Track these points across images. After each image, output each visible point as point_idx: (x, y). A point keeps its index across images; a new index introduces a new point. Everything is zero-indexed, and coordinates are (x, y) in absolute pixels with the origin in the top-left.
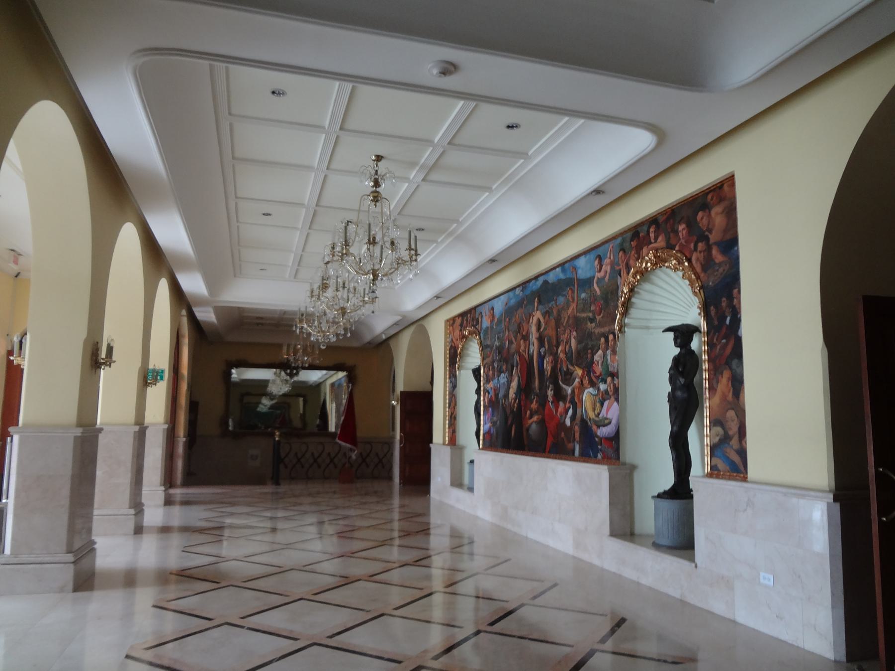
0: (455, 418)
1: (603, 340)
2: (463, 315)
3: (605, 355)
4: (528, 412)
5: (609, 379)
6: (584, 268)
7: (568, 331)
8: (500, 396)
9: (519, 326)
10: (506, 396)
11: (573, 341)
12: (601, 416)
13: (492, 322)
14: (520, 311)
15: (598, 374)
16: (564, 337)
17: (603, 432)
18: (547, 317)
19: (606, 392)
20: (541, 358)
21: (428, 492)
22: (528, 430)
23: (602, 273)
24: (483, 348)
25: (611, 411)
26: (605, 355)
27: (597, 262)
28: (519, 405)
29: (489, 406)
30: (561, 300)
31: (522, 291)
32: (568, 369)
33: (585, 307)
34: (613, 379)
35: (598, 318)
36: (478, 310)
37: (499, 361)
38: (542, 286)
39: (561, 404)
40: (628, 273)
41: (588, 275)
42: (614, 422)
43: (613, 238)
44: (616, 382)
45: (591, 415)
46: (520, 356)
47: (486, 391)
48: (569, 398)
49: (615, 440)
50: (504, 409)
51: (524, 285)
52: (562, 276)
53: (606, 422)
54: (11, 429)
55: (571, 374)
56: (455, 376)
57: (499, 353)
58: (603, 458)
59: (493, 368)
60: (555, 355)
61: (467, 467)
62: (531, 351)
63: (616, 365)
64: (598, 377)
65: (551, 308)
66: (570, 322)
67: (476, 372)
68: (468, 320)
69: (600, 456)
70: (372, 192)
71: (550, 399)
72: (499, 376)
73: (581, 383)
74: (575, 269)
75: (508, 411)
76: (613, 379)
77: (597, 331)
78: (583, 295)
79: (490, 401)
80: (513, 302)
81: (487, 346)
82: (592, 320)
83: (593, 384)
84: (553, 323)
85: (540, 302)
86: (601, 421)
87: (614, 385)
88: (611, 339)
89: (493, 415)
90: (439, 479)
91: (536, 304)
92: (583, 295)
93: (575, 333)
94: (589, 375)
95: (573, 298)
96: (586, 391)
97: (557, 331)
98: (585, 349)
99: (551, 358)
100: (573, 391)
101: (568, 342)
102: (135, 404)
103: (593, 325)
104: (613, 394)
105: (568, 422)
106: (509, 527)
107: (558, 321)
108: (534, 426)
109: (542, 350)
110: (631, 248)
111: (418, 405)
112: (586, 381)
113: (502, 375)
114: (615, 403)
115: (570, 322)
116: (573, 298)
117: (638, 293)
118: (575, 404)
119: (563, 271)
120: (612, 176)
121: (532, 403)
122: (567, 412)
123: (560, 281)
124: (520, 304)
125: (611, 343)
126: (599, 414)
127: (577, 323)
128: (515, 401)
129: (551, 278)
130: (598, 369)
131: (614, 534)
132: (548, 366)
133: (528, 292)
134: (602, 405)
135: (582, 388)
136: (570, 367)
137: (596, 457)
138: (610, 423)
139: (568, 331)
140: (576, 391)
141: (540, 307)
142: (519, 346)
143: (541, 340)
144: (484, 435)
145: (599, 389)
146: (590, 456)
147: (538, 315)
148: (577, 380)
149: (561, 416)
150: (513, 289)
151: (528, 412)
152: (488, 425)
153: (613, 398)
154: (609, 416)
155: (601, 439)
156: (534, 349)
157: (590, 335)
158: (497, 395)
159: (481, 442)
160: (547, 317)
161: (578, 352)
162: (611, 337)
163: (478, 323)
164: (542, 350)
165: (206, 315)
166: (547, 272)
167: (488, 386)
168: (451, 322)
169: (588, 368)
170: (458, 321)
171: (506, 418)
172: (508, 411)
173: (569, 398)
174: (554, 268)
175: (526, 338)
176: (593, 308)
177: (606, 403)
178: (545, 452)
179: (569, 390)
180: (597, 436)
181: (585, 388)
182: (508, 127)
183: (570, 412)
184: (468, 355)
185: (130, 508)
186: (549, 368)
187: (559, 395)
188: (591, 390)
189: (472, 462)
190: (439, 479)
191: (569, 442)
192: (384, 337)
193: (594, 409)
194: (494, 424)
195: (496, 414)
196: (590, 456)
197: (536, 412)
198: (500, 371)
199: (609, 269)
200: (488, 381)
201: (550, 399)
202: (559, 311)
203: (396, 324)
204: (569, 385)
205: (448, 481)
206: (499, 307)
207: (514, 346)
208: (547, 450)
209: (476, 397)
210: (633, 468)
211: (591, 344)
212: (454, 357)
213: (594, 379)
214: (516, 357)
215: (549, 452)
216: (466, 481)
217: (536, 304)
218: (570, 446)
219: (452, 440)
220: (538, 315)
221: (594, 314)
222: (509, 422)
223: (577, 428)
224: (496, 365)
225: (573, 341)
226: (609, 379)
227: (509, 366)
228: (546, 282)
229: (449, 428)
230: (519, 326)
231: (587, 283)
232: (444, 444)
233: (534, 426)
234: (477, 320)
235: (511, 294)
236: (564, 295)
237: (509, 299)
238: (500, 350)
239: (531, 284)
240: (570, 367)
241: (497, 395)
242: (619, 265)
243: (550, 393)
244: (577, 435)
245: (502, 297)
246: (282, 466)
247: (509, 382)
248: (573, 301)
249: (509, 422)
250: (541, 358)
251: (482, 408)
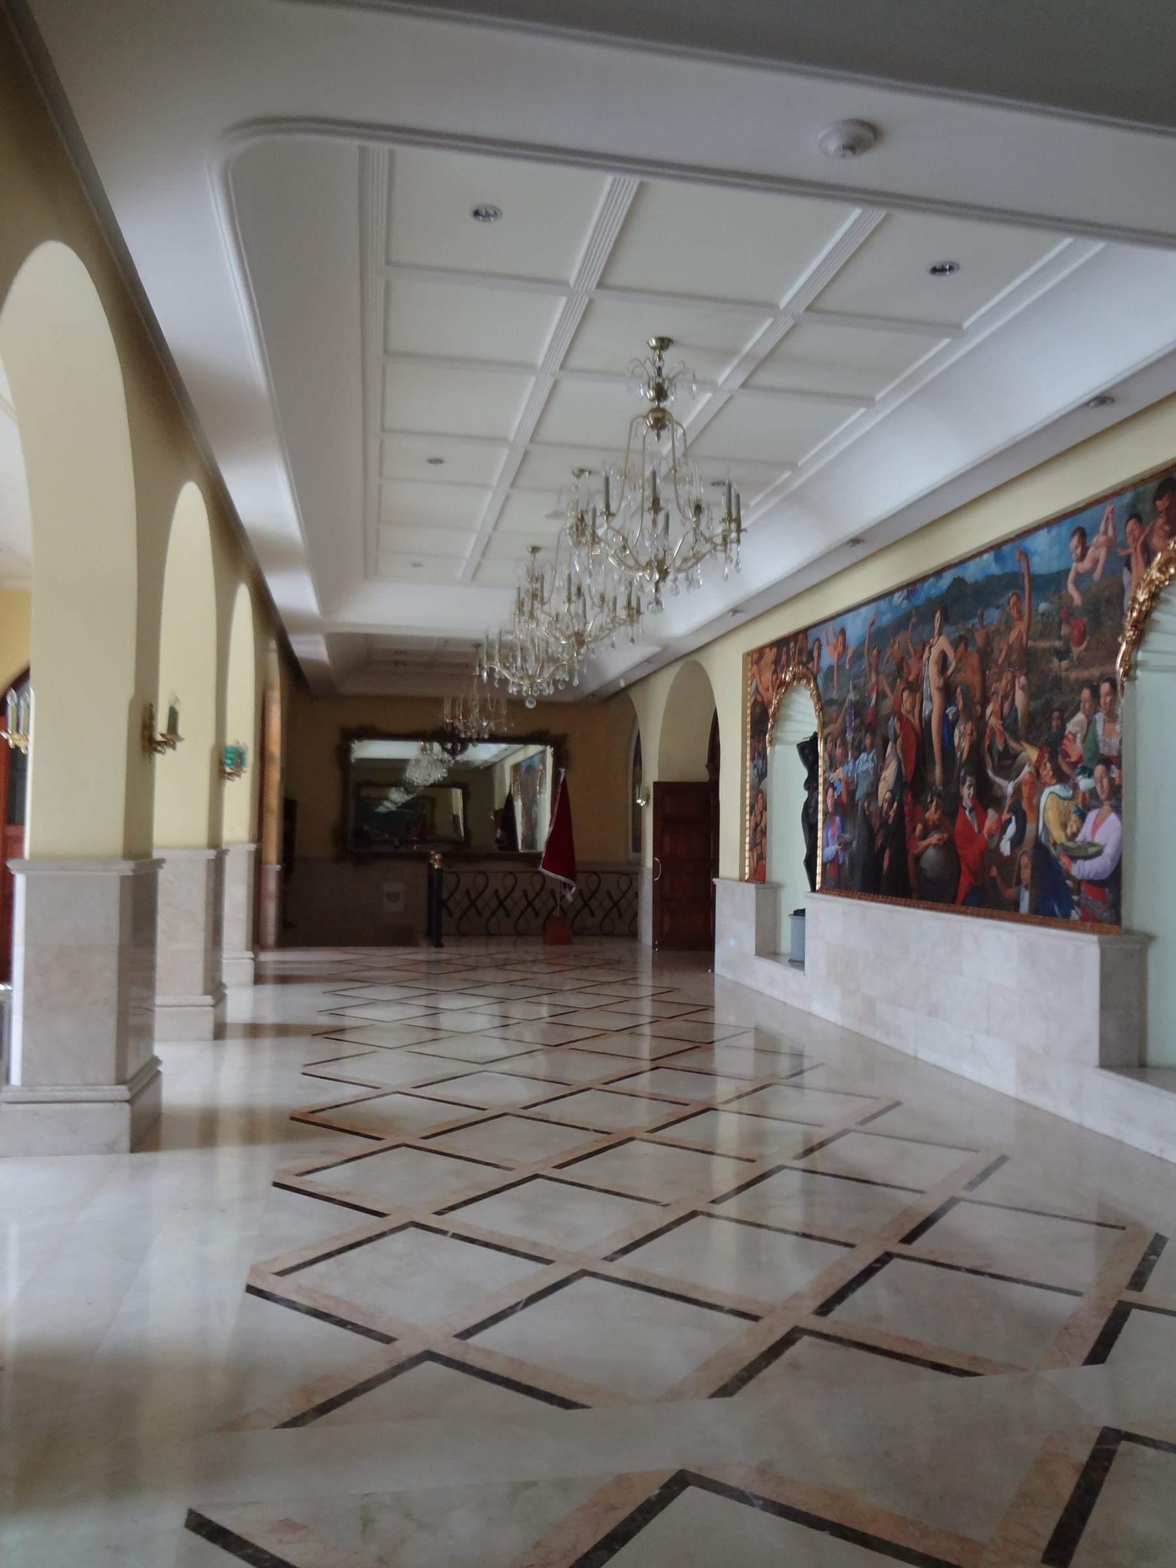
0: (764, 833)
1: (1086, 693)
2: (780, 644)
3: (1090, 722)
4: (919, 827)
5: (1099, 770)
6: (1045, 554)
7: (1008, 676)
8: (859, 794)
9: (901, 666)
10: (872, 794)
11: (1020, 697)
12: (1080, 838)
13: (841, 656)
14: (901, 637)
15: (1074, 759)
16: (1001, 686)
17: (1083, 869)
18: (961, 648)
19: (1093, 793)
20: (948, 726)
21: (708, 962)
22: (918, 859)
23: (1087, 564)
24: (824, 705)
25: (1104, 830)
26: (1090, 722)
27: (1075, 541)
28: (900, 812)
29: (835, 813)
30: (993, 615)
31: (908, 597)
32: (1006, 746)
33: (1048, 627)
34: (1108, 769)
35: (1076, 651)
36: (812, 635)
37: (856, 730)
38: (949, 589)
39: (991, 813)
40: (1148, 563)
41: (1055, 567)
42: (1109, 851)
43: (1116, 493)
44: (1115, 774)
45: (1058, 835)
46: (901, 718)
47: (829, 785)
48: (1008, 802)
49: (1112, 885)
50: (867, 819)
51: (911, 587)
52: (995, 569)
53: (1092, 850)
54: (11, 864)
55: (1016, 756)
56: (764, 756)
57: (858, 714)
58: (1084, 918)
59: (844, 742)
60: (980, 722)
61: (787, 925)
62: (926, 712)
63: (1115, 741)
64: (1074, 765)
65: (971, 632)
66: (1014, 658)
67: (808, 751)
68: (791, 655)
69: (1075, 915)
70: (653, 410)
71: (967, 802)
72: (856, 758)
73: (1037, 774)
74: (1025, 555)
75: (876, 823)
76: (1108, 769)
77: (1073, 675)
78: (1043, 606)
79: (838, 803)
80: (886, 619)
81: (831, 702)
82: (1063, 654)
83: (1061, 777)
84: (974, 660)
85: (945, 619)
86: (1079, 848)
87: (1111, 780)
88: (1107, 691)
89: (843, 831)
90: (732, 942)
91: (937, 624)
92: (1043, 606)
93: (1023, 679)
94: (1053, 758)
95: (1019, 612)
96: (1047, 791)
97: (984, 675)
98: (1047, 710)
99: (969, 726)
100: (1017, 790)
101: (1008, 695)
102: (209, 815)
103: (1065, 663)
104: (1108, 799)
105: (1005, 848)
106: (878, 1036)
107: (986, 657)
108: (931, 852)
109: (951, 711)
110: (1155, 512)
111: (690, 809)
112: (1047, 771)
113: (864, 756)
114: (1113, 817)
115: (1014, 658)
116: (1019, 612)
117: (1167, 601)
119: (999, 559)
120: (1143, 365)
121: (927, 810)
122: (1004, 830)
123: (990, 578)
124: (902, 623)
125: (1105, 699)
126: (1075, 835)
127: (1028, 661)
129: (972, 573)
130: (1076, 749)
131: (1106, 1064)
132: (962, 739)
133: (920, 599)
134: (1083, 817)
135: (1037, 783)
136: (1013, 744)
137: (1067, 916)
138: (1099, 853)
139: (1008, 676)
140: (1025, 790)
141: (947, 628)
142: (899, 702)
143: (948, 692)
144: (824, 865)
145: (1075, 787)
146: (1055, 916)
147: (941, 644)
148: (1027, 769)
149: (991, 835)
150: (888, 595)
151: (919, 827)
152: (833, 849)
153: (1107, 807)
154: (1097, 840)
155: (1079, 882)
156: (933, 707)
157: (1058, 683)
158: (851, 793)
159: (819, 879)
160: (961, 648)
161: (1031, 716)
162: (1105, 687)
163: (810, 658)
164: (951, 711)
165: (311, 649)
166: (962, 562)
167: (834, 776)
168: (756, 657)
169: (1053, 747)
170: (770, 655)
171: (872, 836)
172: (876, 823)
173: (1008, 802)
174: (979, 554)
175: (915, 687)
176: (1065, 631)
177: (1092, 816)
178: (953, 902)
179: (1009, 788)
180: (1071, 877)
181: (1046, 785)
182: (935, 270)
183: (1012, 829)
184: (788, 718)
185: (206, 993)
186: (965, 745)
187: (987, 796)
188: (1057, 788)
189: (800, 913)
190: (732, 942)
191: (1009, 886)
192: (622, 684)
193: (1064, 826)
194: (845, 846)
195: (849, 827)
196: (1055, 916)
197: (937, 827)
198: (859, 750)
199: (1102, 553)
200: (832, 766)
201: (967, 802)
202: (987, 634)
203: (648, 661)
204: (1009, 778)
205: (750, 944)
206: (856, 629)
207: (888, 704)
208: (961, 896)
209: (805, 795)
210: (1148, 939)
211: (1058, 701)
212: (761, 722)
213: (1065, 768)
214: (894, 723)
215: (964, 903)
216: (786, 944)
217: (937, 624)
218: (1010, 892)
219: (759, 873)
220: (941, 644)
221: (1067, 642)
222: (879, 842)
223: (1025, 861)
224: (849, 736)
225: (1020, 697)
226: (1099, 770)
227: (878, 740)
228: (959, 582)
229: (750, 850)
230: (901, 666)
231: (1053, 582)
232: (741, 879)
233: (931, 852)
234: (811, 653)
235: (883, 604)
236: (997, 607)
237: (879, 614)
238: (858, 709)
239: (926, 585)
240: (1013, 744)
241: (851, 793)
242: (1124, 545)
243: (967, 792)
244: (1026, 874)
245: (863, 610)
246: (444, 914)
248: (1021, 618)
249: (879, 842)
250: (948, 726)
251: (820, 817)
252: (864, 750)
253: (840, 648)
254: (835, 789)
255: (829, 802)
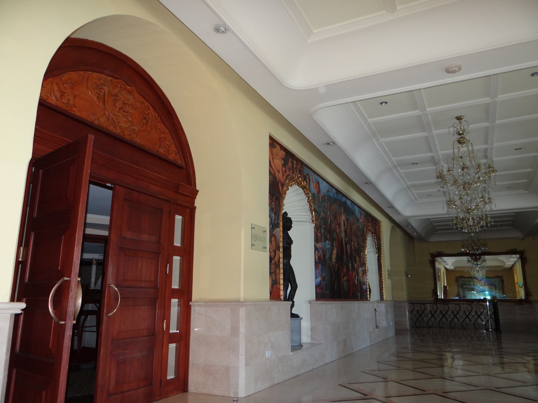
10: (331, 258)
16: (353, 238)
28: (338, 267)
51: (338, 192)
59: (321, 232)
72: (325, 242)
79: (319, 258)
101: (354, 242)
108: (345, 283)
118: (358, 273)
128: (336, 263)
129: (349, 202)
156: (343, 235)
169: (360, 257)
175: (339, 225)
207: (333, 226)
228: (345, 202)
238: (325, 220)
243: (350, 265)
247: (332, 250)
252: (327, 240)
253: (318, 189)
254: (318, 252)
255: (316, 256)
